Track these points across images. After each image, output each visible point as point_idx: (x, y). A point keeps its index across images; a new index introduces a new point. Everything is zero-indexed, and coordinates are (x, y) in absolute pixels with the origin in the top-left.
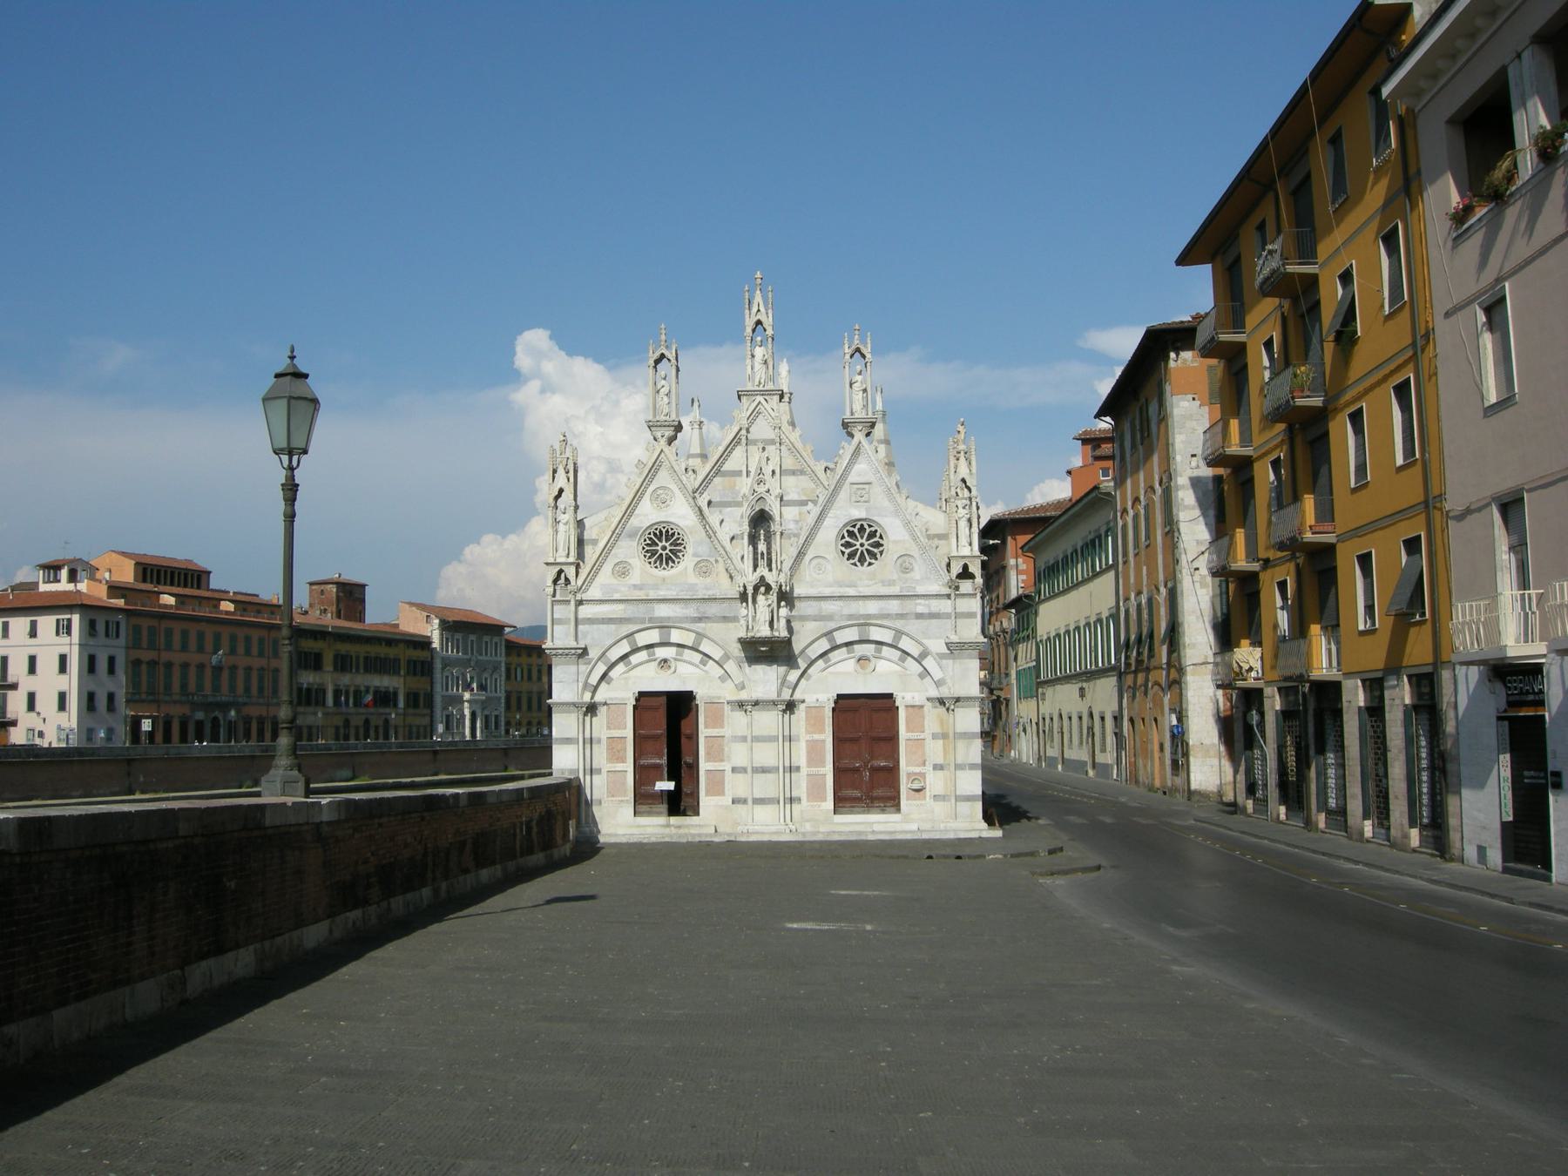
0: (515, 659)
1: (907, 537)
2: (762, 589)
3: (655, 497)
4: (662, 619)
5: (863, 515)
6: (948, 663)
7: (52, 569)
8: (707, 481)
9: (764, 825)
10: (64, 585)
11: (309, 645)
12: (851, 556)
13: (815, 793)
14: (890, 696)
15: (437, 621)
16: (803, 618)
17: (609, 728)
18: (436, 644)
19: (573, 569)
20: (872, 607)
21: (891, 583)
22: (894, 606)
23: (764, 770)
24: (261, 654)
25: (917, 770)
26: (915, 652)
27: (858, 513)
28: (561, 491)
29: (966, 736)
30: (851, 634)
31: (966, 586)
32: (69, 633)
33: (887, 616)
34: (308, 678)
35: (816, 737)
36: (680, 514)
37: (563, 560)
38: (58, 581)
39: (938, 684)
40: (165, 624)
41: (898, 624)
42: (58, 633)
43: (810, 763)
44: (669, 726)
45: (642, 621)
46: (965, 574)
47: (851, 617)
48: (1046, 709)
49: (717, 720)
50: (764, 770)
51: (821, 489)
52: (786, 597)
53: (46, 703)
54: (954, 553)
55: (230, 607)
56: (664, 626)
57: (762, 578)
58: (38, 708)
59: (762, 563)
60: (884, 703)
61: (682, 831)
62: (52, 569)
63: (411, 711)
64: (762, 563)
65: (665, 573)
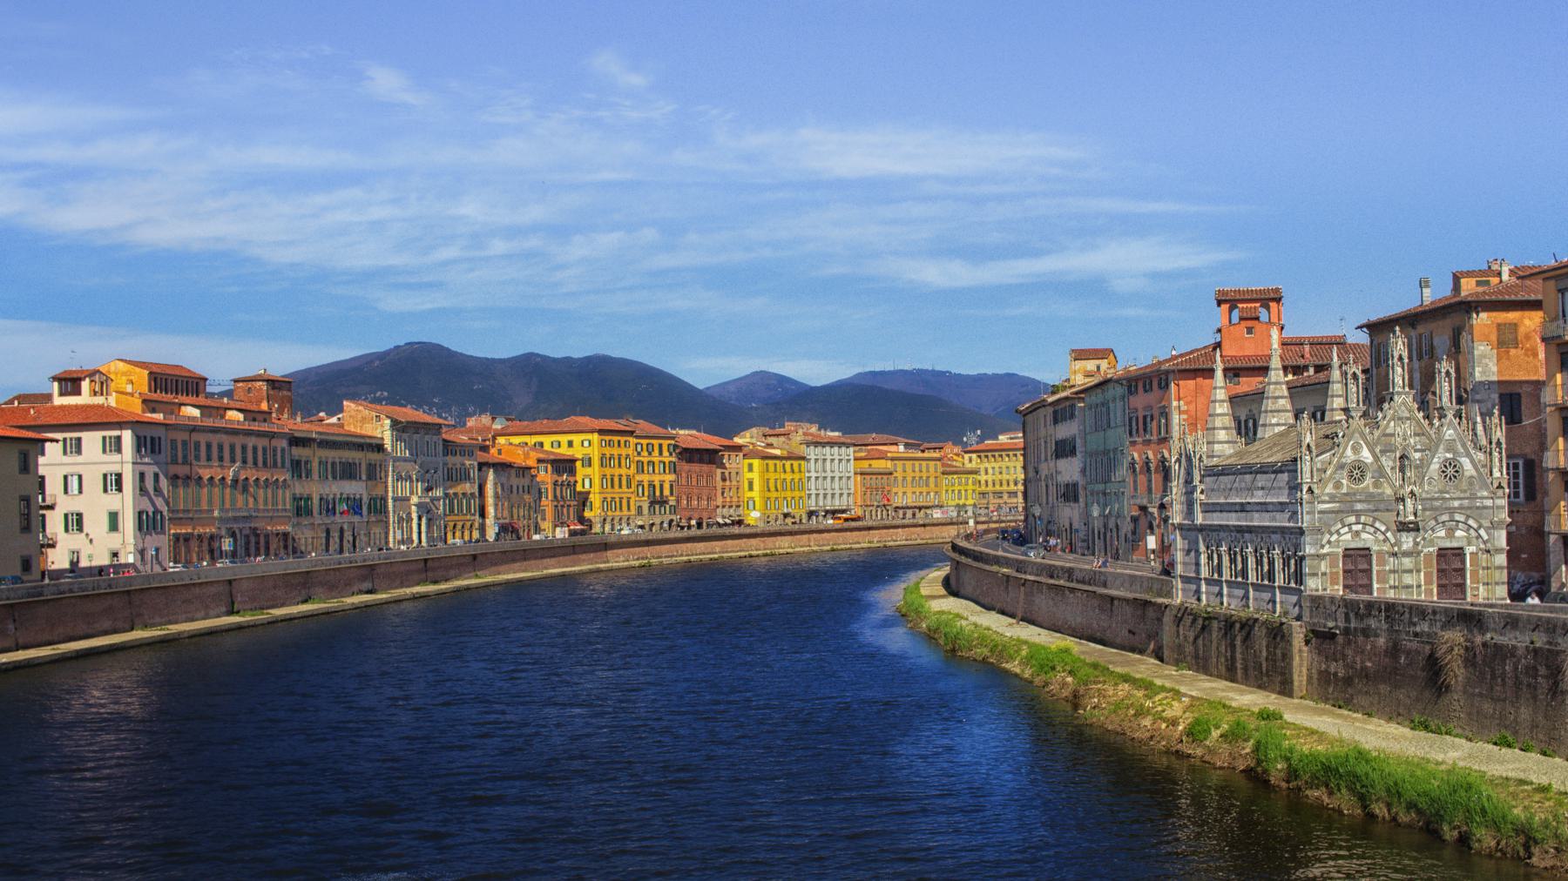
3: (1353, 448)
7: (70, 383)
10: (85, 398)
15: (388, 422)
18: (388, 447)
29: (1500, 568)
30: (1445, 518)
31: (1500, 492)
32: (119, 450)
34: (300, 488)
38: (78, 392)
39: (1485, 542)
40: (196, 437)
42: (104, 451)
44: (1357, 562)
46: (1500, 487)
49: (1382, 562)
53: (96, 524)
55: (241, 417)
56: (1358, 514)
58: (86, 529)
60: (1459, 553)
62: (70, 383)
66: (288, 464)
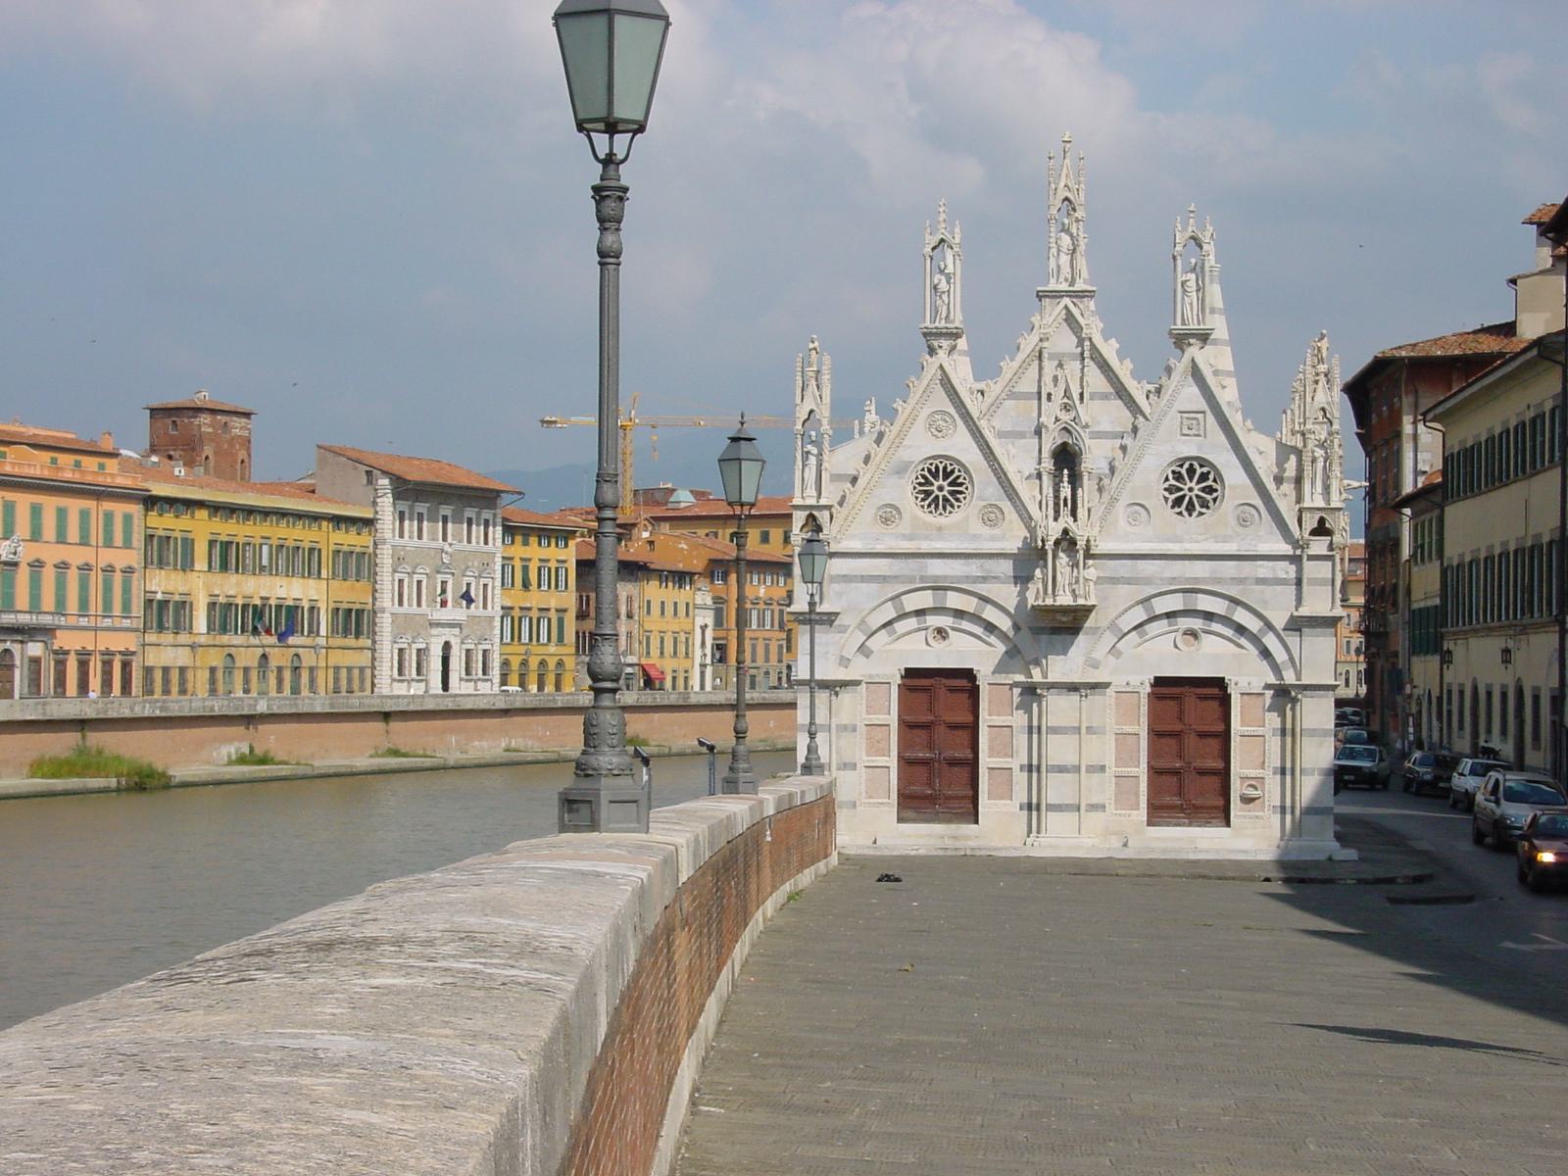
0: (518, 550)
1: (1248, 482)
2: (1064, 544)
4: (936, 578)
5: (1194, 453)
6: (1293, 640)
8: (996, 404)
9: (1066, 838)
11: (164, 522)
12: (1178, 502)
13: (1124, 798)
14: (1223, 678)
16: (1114, 581)
17: (868, 713)
19: (826, 513)
20: (1201, 569)
21: (1225, 539)
22: (1229, 568)
23: (1061, 769)
24: (84, 542)
25: (1253, 773)
26: (1253, 624)
27: (1189, 449)
28: (811, 412)
31: (1319, 546)
33: (1219, 581)
34: (163, 583)
35: (1128, 729)
36: (960, 446)
37: (812, 502)
41: (1233, 592)
43: (1120, 761)
45: (912, 580)
46: (1321, 530)
47: (1173, 580)
48: (1455, 675)
50: (1061, 769)
51: (1141, 419)
52: (1088, 555)
54: (1307, 504)
57: (1066, 532)
59: (1065, 512)
61: (958, 844)
63: (339, 641)
64: (1065, 512)
65: (942, 520)
66: (138, 540)
